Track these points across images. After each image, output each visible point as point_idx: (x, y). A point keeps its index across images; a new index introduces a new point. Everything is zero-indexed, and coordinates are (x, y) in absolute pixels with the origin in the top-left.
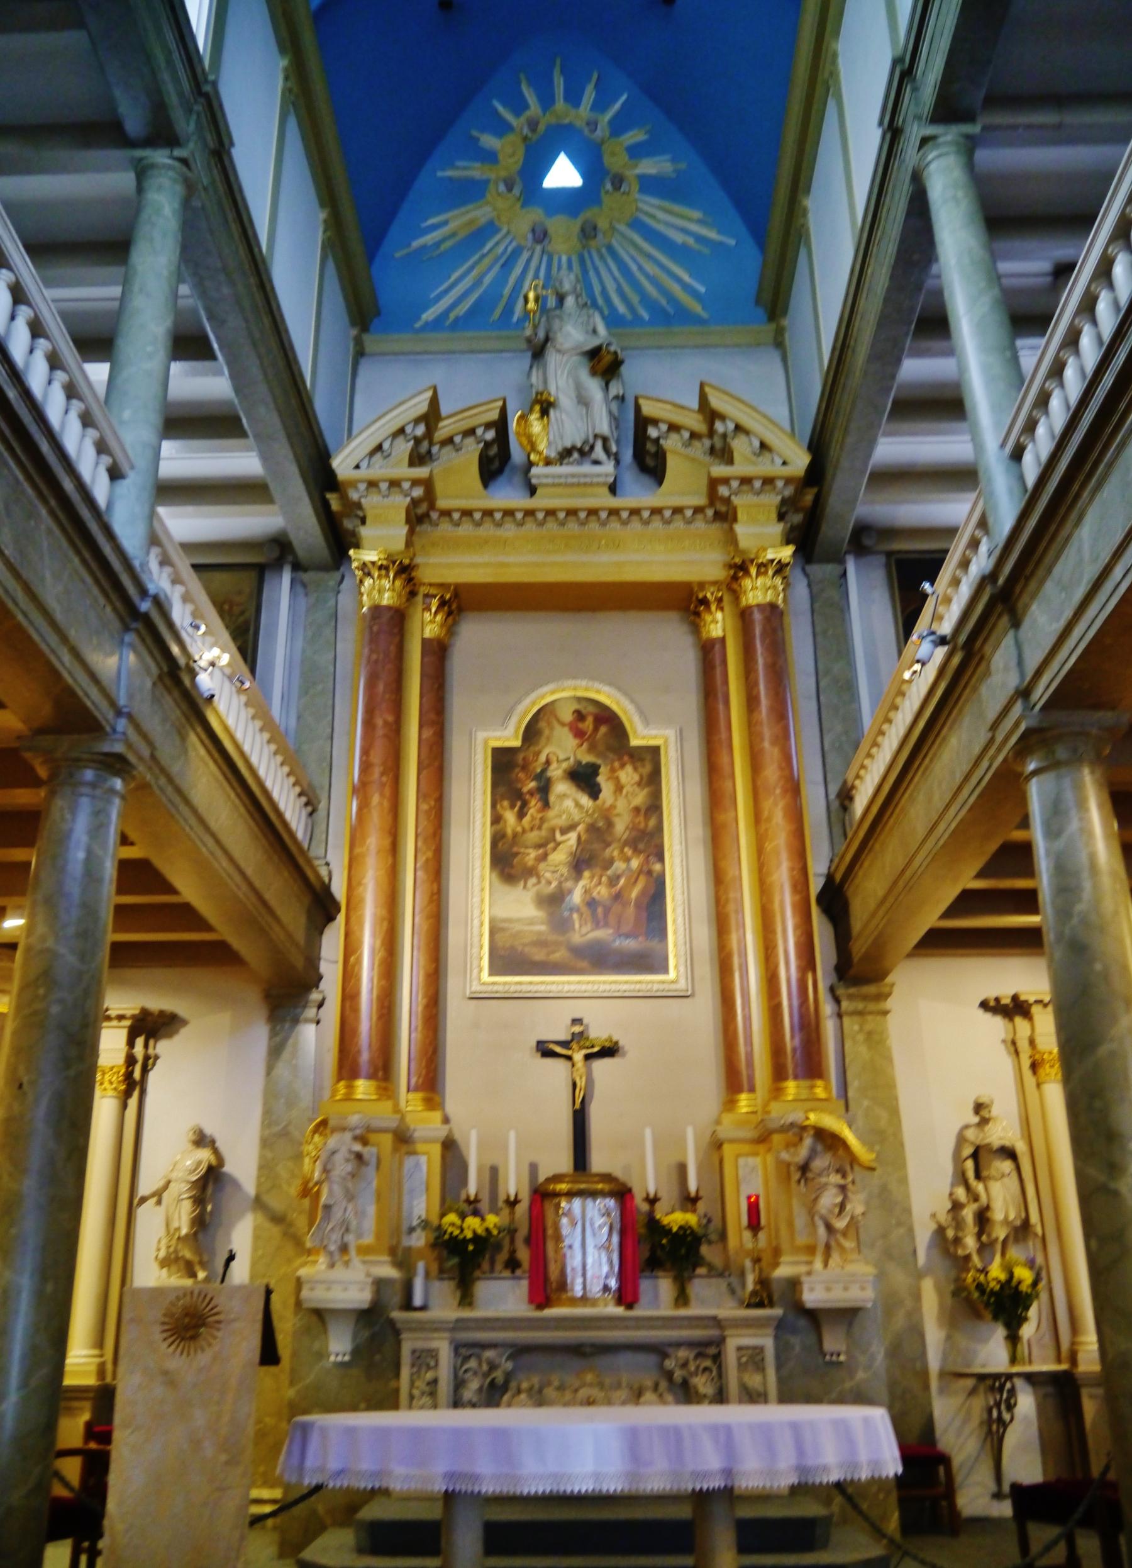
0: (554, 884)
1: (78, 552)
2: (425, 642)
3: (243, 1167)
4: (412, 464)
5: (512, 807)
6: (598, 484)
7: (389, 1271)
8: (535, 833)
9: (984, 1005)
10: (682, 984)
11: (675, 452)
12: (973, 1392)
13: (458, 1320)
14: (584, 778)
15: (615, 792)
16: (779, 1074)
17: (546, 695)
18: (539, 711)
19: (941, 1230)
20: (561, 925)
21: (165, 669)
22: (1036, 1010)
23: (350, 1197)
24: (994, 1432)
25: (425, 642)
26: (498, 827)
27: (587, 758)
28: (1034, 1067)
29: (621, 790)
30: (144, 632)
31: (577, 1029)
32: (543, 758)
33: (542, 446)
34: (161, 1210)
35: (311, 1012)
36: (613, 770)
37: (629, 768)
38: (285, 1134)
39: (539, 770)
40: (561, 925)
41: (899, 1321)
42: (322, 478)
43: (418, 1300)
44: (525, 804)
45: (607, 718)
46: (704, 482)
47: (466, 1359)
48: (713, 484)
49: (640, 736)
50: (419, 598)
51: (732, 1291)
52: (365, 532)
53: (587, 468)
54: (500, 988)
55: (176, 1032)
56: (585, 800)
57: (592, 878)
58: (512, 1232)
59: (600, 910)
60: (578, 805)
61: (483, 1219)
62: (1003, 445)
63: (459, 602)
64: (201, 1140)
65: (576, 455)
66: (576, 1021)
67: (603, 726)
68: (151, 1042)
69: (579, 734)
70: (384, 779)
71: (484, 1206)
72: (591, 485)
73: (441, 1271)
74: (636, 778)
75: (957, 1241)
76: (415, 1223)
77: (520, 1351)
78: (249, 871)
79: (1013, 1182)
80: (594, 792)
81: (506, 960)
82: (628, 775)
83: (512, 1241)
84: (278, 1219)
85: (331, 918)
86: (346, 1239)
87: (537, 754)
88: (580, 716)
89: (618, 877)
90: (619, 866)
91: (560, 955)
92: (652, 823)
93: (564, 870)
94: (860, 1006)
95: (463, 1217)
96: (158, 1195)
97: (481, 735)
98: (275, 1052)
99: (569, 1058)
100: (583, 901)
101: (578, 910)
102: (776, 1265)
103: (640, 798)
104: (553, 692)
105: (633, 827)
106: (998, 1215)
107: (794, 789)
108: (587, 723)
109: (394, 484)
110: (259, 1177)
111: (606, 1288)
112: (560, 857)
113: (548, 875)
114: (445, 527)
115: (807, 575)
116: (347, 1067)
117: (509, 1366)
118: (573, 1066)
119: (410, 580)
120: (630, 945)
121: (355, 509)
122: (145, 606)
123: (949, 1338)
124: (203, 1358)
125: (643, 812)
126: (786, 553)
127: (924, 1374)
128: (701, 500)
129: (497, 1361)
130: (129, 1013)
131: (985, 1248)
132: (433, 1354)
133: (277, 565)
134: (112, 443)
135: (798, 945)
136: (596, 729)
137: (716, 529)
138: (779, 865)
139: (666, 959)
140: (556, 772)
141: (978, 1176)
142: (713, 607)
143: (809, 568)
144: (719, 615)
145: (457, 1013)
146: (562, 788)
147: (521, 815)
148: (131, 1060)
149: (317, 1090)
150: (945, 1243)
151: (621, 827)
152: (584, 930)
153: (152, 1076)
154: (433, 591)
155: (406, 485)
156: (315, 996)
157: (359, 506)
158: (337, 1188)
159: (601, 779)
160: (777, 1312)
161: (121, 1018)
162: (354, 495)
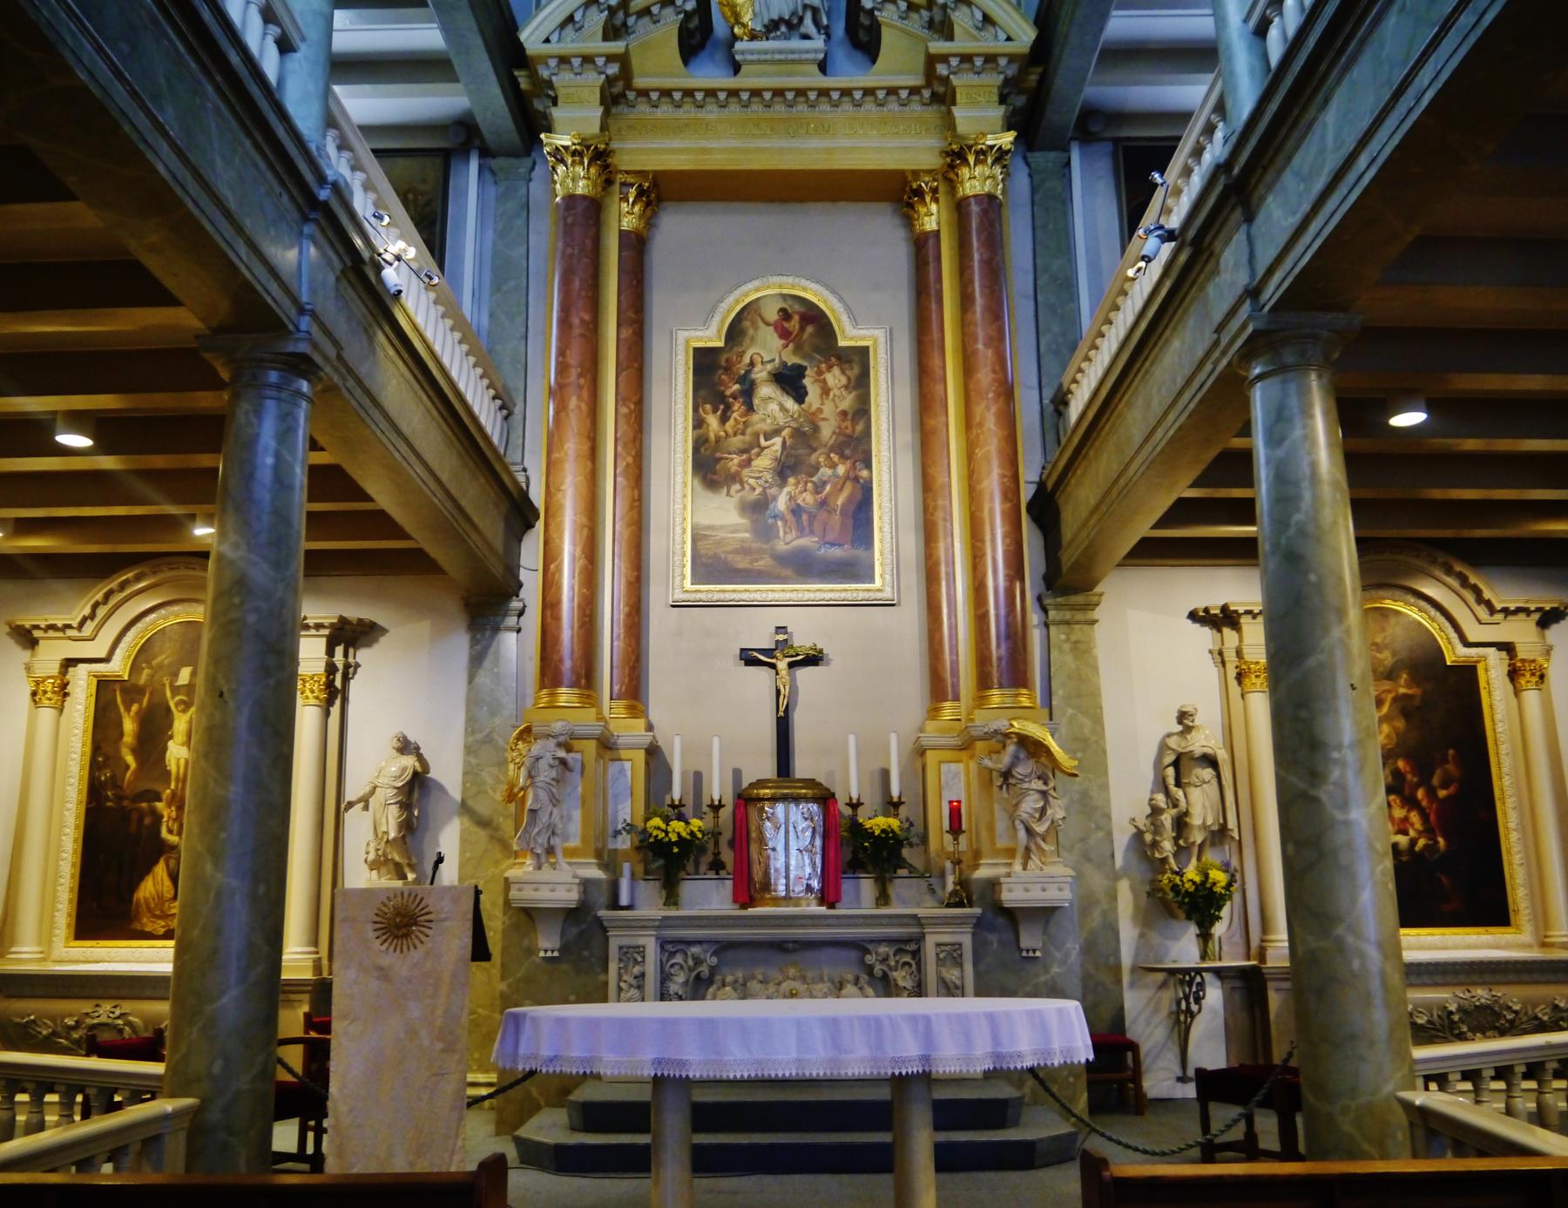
0: (759, 490)
1: (249, 134)
2: (622, 234)
3: (448, 771)
4: (606, 38)
5: (715, 411)
6: (807, 61)
7: (595, 873)
8: (740, 437)
9: (1193, 616)
10: (888, 594)
11: (889, 25)
12: (1163, 986)
13: (665, 918)
14: (790, 381)
16: (984, 682)
17: (750, 292)
18: (743, 310)
19: (1139, 834)
20: (765, 532)
21: (349, 263)
22: (1244, 620)
23: (555, 801)
24: (1181, 1022)
25: (622, 234)
26: (700, 431)
27: (792, 360)
28: (1240, 677)
29: (828, 393)
30: (323, 222)
31: (781, 637)
32: (747, 360)
33: (747, 18)
34: (369, 815)
35: (511, 621)
36: (820, 373)
37: (836, 370)
38: (489, 740)
40: (765, 532)
41: (1096, 918)
42: (509, 54)
43: (624, 901)
44: (728, 407)
45: (814, 318)
46: (922, 59)
47: (672, 954)
48: (932, 60)
50: (616, 187)
51: (932, 891)
52: (557, 113)
53: (796, 43)
55: (376, 640)
56: (790, 404)
57: (797, 484)
58: (716, 835)
59: (805, 517)
60: (783, 409)
61: (687, 823)
62: (1246, 21)
63: (659, 191)
64: (405, 747)
65: (783, 29)
66: (781, 629)
67: (809, 326)
68: (351, 651)
69: (784, 334)
70: (582, 381)
71: (688, 810)
72: (800, 62)
73: (647, 872)
74: (844, 380)
75: (1155, 845)
76: (620, 827)
77: (724, 948)
78: (444, 477)
79: (1213, 789)
80: (800, 395)
81: (709, 567)
82: (835, 378)
83: (717, 844)
84: (483, 823)
85: (530, 526)
87: (741, 355)
88: (785, 314)
89: (824, 483)
90: (826, 472)
91: (764, 563)
92: (860, 427)
93: (768, 476)
94: (1068, 615)
95: (667, 820)
96: (365, 801)
97: (682, 335)
98: (476, 660)
101: (783, 519)
102: (976, 866)
103: (848, 402)
104: (757, 290)
105: (839, 432)
106: (1196, 820)
107: (1007, 392)
109: (588, 59)
110: (464, 783)
111: (809, 888)
112: (764, 462)
113: (752, 481)
114: (643, 108)
115: (1028, 164)
116: (549, 675)
117: (714, 960)
119: (606, 167)
120: (837, 553)
121: (545, 88)
122: (324, 194)
123: (1142, 935)
124: (416, 955)
126: (1007, 139)
127: (1117, 969)
128: (917, 81)
130: (326, 622)
131: (1181, 851)
132: (641, 950)
133: (463, 152)
134: (280, 12)
135: (1005, 552)
136: (802, 329)
137: (932, 114)
138: (990, 472)
139: (872, 567)
140: (760, 374)
141: (1178, 784)
142: (928, 199)
143: (1029, 155)
144: (934, 207)
145: (660, 620)
146: (766, 390)
147: (724, 419)
148: (331, 669)
149: (520, 696)
150: (1142, 846)
151: (827, 431)
152: (789, 537)
153: (354, 685)
154: (630, 180)
155: (600, 61)
156: (515, 604)
157: (549, 84)
158: (543, 795)
159: (807, 381)
160: (977, 911)
161: (318, 626)
162: (544, 73)
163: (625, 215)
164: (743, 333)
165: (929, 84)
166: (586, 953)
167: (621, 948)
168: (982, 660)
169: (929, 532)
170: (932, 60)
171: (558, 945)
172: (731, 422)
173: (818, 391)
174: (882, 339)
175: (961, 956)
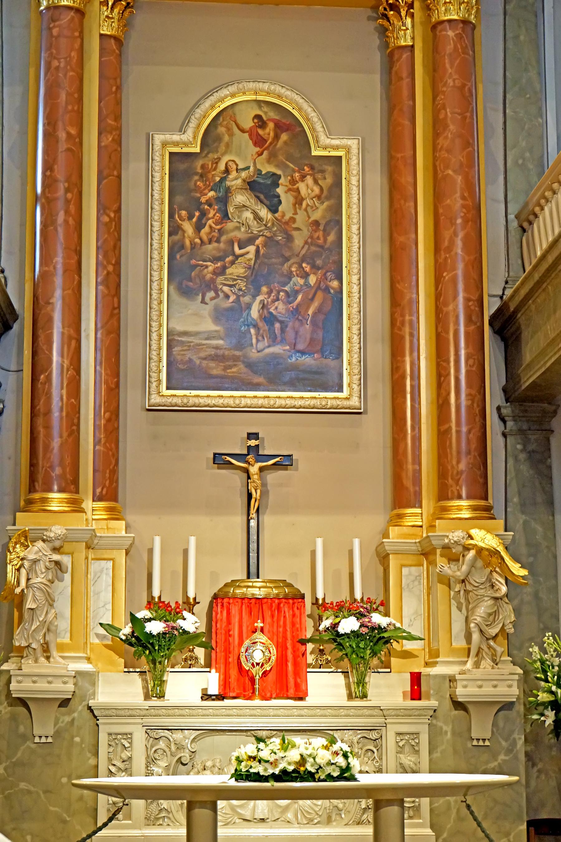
8: (215, 245)
10: (355, 402)
14: (263, 189)
15: (294, 205)
16: (444, 494)
26: (176, 238)
27: (266, 168)
31: (253, 443)
32: (222, 167)
36: (293, 182)
37: (309, 180)
39: (218, 179)
44: (203, 214)
45: (288, 125)
49: (324, 144)
54: (179, 401)
56: (264, 212)
57: (269, 293)
59: (277, 325)
60: (257, 217)
66: (252, 436)
69: (259, 141)
70: (69, 195)
74: (317, 190)
82: (307, 188)
86: (47, 638)
88: (260, 121)
89: (297, 292)
92: (331, 238)
97: (158, 138)
99: (247, 471)
100: (260, 316)
101: (255, 326)
104: (233, 95)
105: (310, 242)
108: (267, 130)
118: (249, 478)
125: (321, 227)
129: (184, 744)
132: (128, 736)
135: (468, 372)
140: (235, 181)
142: (403, 13)
146: (240, 198)
147: (199, 227)
152: (260, 346)
164: (219, 139)
166: (77, 739)
167: (110, 734)
169: (398, 344)
172: (206, 229)
173: (292, 200)
174: (354, 151)
175: (418, 744)
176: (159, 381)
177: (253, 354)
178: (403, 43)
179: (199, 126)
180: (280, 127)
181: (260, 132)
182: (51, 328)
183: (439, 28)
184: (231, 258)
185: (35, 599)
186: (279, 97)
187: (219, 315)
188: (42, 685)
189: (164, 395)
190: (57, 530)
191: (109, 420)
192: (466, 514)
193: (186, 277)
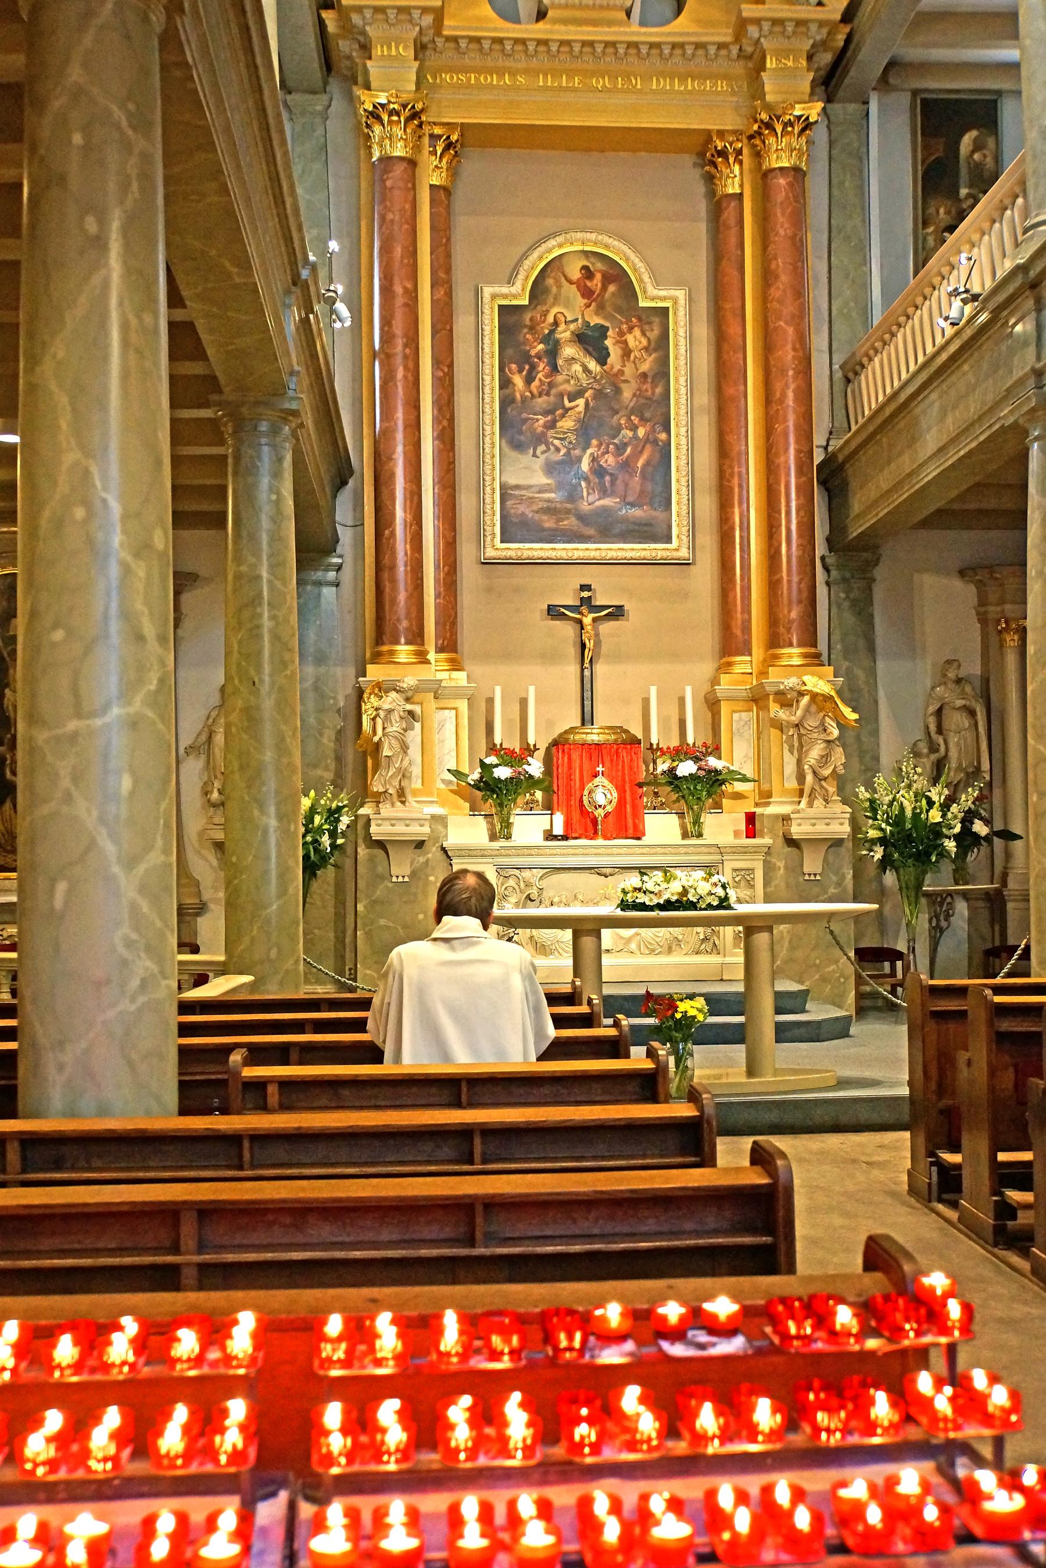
0: (563, 451)
8: (545, 398)
10: (684, 553)
14: (591, 341)
15: (623, 357)
16: (774, 641)
17: (553, 249)
26: (507, 391)
27: (595, 320)
31: (585, 594)
32: (550, 319)
36: (621, 334)
37: (637, 332)
39: (547, 332)
40: (573, 496)
44: (533, 367)
45: (616, 275)
48: (742, 24)
56: (593, 365)
57: (599, 446)
59: (607, 478)
60: (586, 370)
66: (585, 587)
67: (609, 283)
69: (587, 293)
70: (407, 351)
74: (644, 342)
80: (602, 358)
82: (635, 339)
87: (545, 314)
91: (570, 523)
93: (572, 437)
97: (488, 291)
101: (586, 479)
104: (560, 246)
105: (638, 394)
113: (557, 442)
120: (636, 513)
126: (814, 111)
128: (725, 35)
135: (798, 523)
136: (604, 288)
140: (564, 334)
141: (940, 731)
142: (731, 160)
146: (569, 351)
152: (591, 498)
154: (437, 131)
155: (416, 14)
163: (433, 173)
164: (546, 291)
165: (737, 39)
168: (773, 621)
169: (725, 496)
170: (742, 24)
171: (408, 873)
172: (536, 383)
174: (682, 302)
176: (493, 534)
177: (584, 507)
178: (730, 191)
179: (527, 278)
180: (607, 279)
181: (589, 284)
182: (394, 484)
183: (770, 176)
184: (559, 412)
185: (391, 747)
186: (607, 246)
187: (550, 469)
188: (400, 828)
189: (497, 548)
190: (409, 681)
191: (448, 574)
192: (797, 661)
193: (515, 432)
